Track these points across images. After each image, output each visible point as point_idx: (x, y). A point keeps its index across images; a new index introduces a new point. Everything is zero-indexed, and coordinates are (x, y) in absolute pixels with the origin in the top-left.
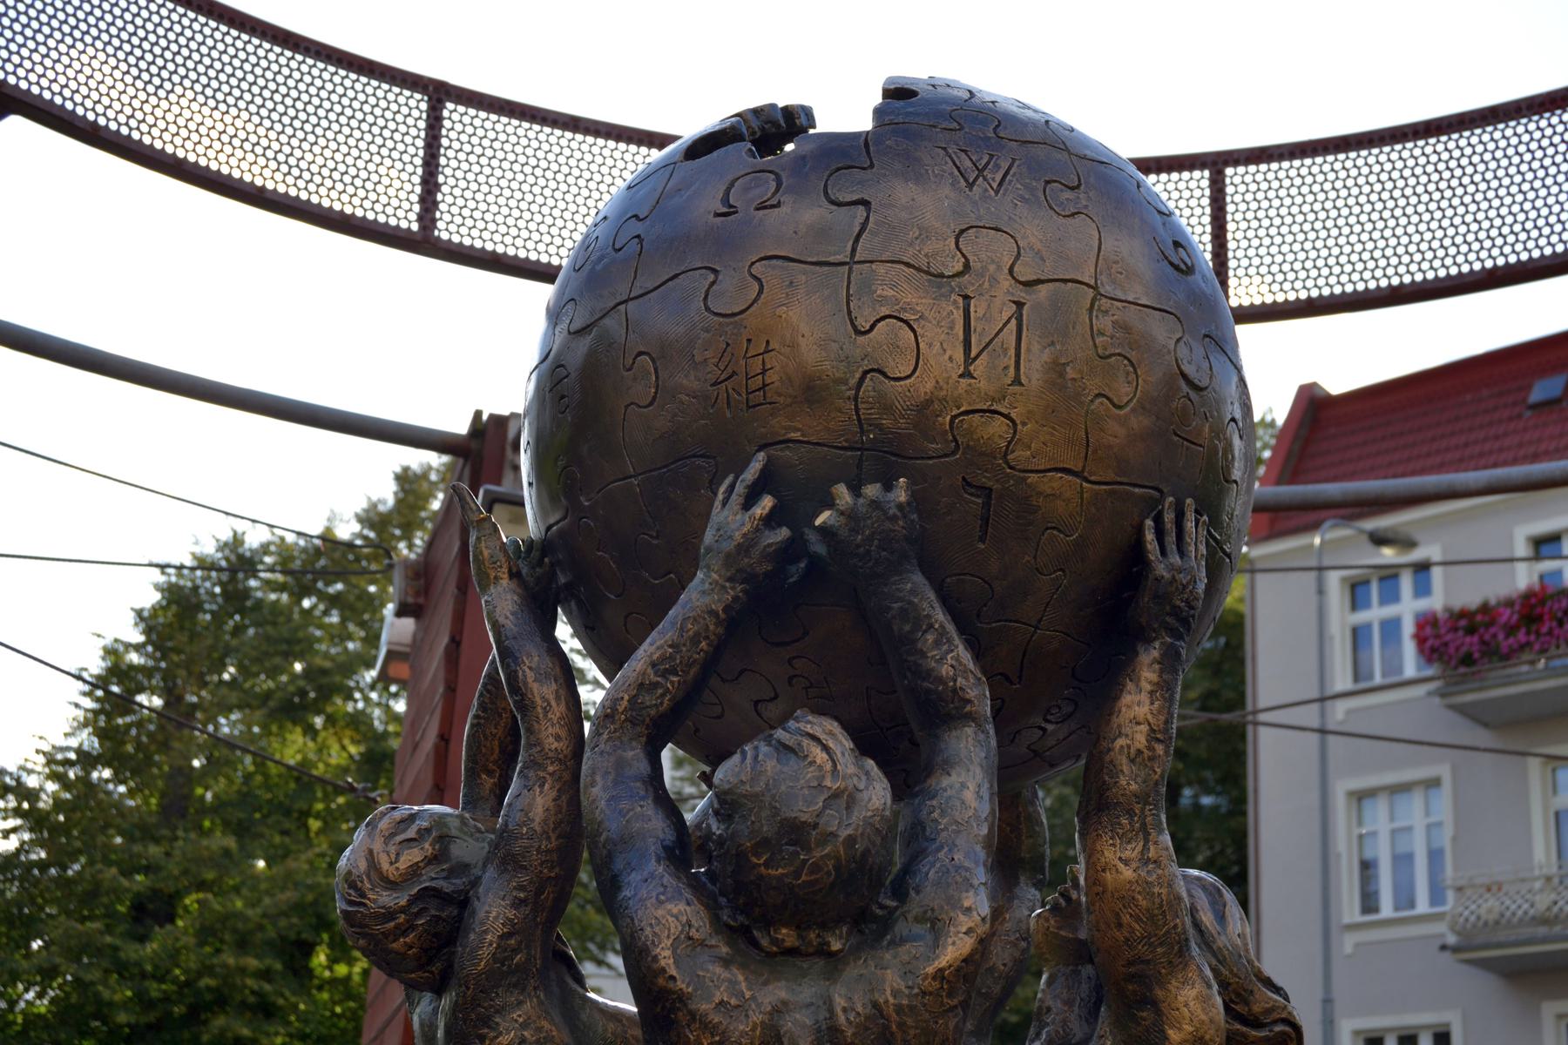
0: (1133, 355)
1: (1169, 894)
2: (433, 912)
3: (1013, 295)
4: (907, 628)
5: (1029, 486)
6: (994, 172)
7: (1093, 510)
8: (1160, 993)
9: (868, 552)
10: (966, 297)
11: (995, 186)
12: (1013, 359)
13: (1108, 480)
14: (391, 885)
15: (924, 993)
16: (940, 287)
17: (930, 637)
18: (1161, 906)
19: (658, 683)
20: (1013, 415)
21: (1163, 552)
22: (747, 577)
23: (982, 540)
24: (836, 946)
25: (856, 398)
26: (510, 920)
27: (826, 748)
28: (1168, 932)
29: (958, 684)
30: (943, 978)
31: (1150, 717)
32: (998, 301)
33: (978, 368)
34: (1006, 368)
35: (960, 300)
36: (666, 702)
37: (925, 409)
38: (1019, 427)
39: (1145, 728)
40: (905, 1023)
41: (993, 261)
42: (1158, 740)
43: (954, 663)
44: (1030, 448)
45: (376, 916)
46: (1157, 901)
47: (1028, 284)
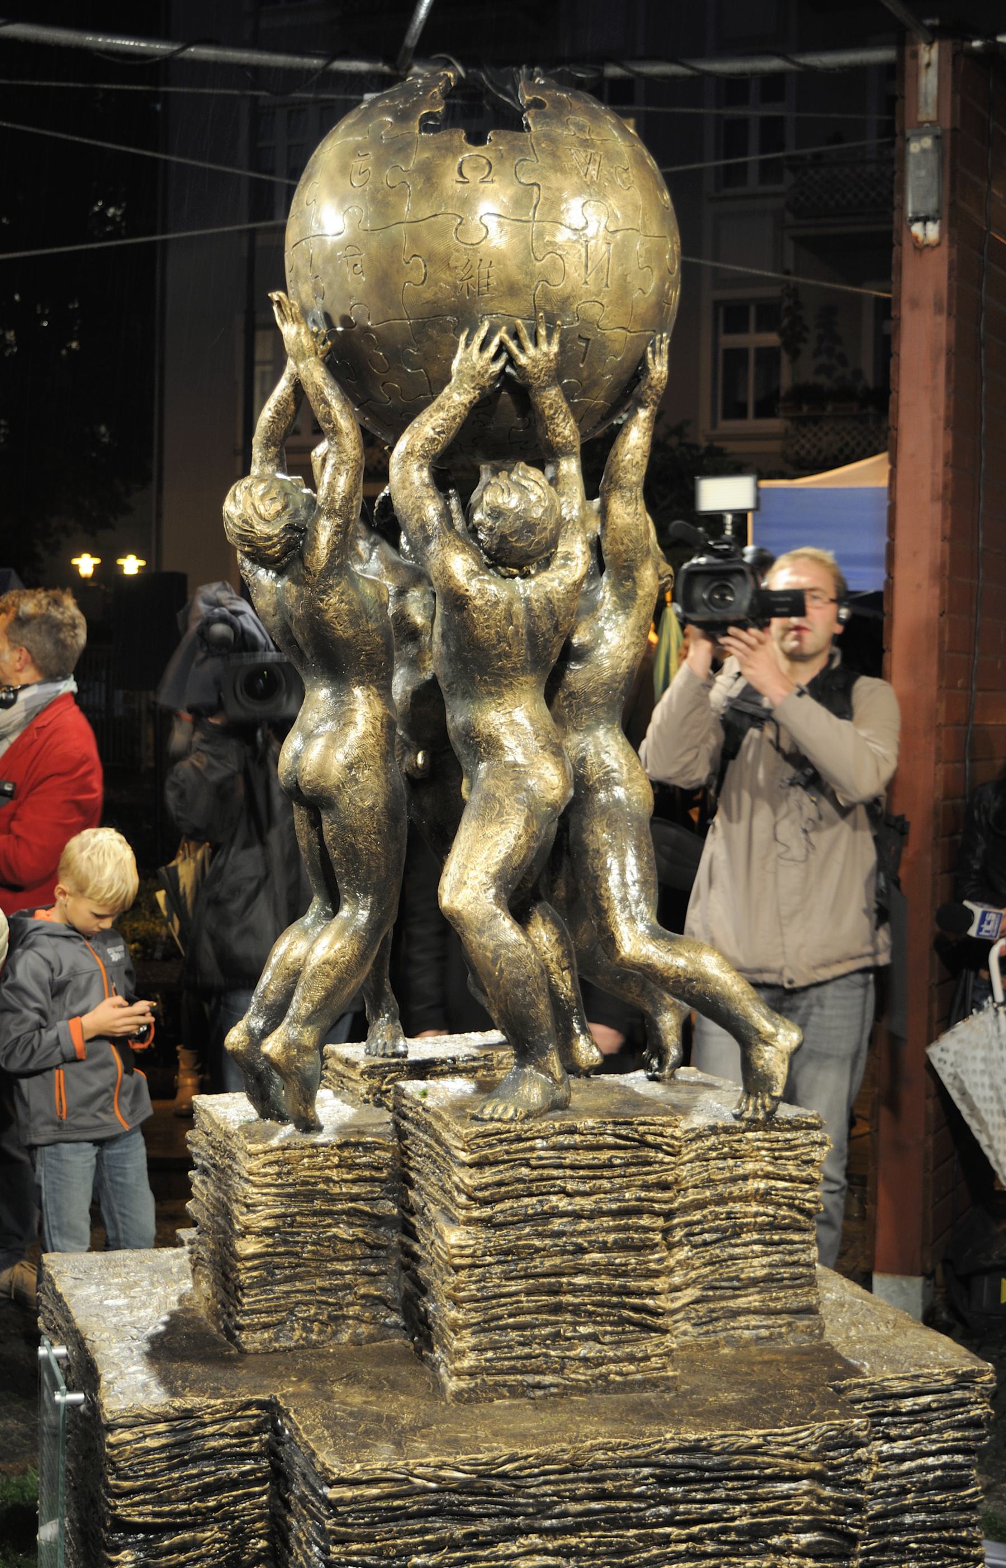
8: (636, 574)
22: (482, 388)
45: (261, 538)
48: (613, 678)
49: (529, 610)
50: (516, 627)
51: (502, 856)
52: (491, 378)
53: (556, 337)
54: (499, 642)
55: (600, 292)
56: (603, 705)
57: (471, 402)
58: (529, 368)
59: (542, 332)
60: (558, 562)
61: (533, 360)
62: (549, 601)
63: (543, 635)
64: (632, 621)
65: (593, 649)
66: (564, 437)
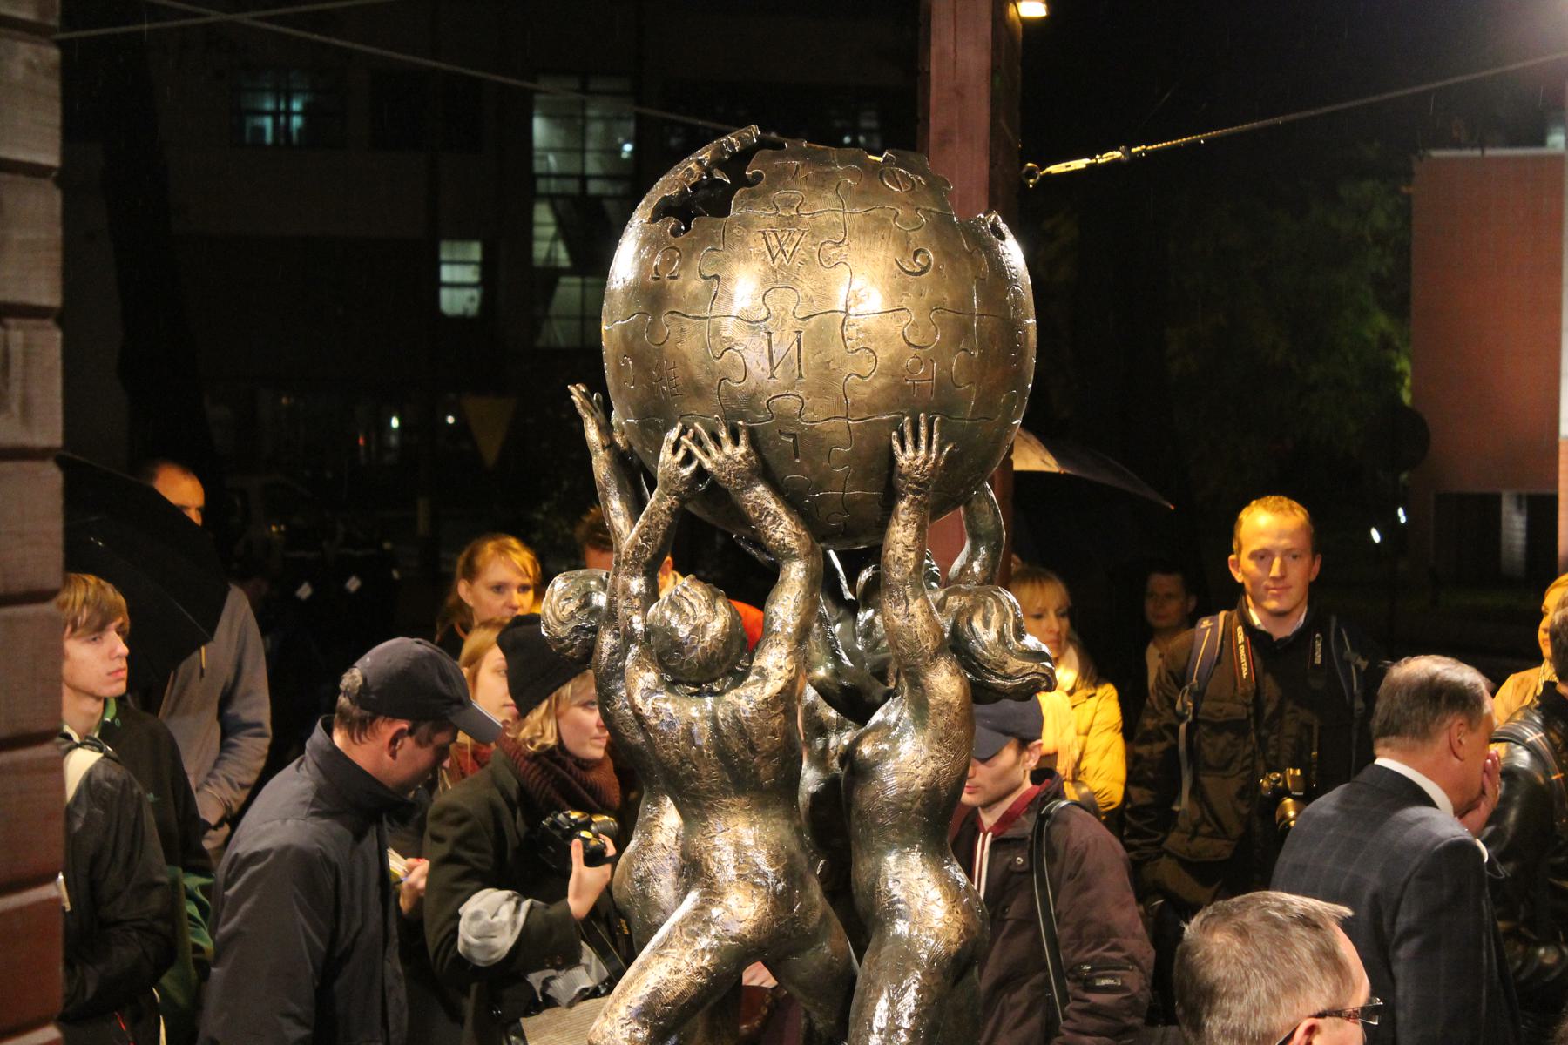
0: (872, 346)
1: (921, 631)
2: (582, 637)
3: (795, 327)
4: (757, 514)
5: (817, 429)
6: (789, 246)
7: (858, 434)
9: (729, 480)
10: (770, 333)
11: (788, 256)
12: (797, 365)
13: (864, 417)
14: (562, 623)
15: (759, 710)
16: (754, 329)
17: (769, 519)
18: (917, 638)
19: (643, 546)
20: (800, 395)
21: (903, 449)
23: (797, 457)
24: (717, 689)
25: (718, 394)
26: (614, 646)
27: (691, 604)
28: (923, 650)
29: (786, 541)
30: (768, 703)
31: (903, 539)
32: (786, 333)
33: (778, 373)
34: (793, 371)
35: (766, 335)
36: (648, 555)
37: (753, 396)
38: (805, 401)
39: (901, 545)
40: (750, 725)
41: (783, 309)
42: (910, 551)
43: (783, 530)
44: (813, 410)
46: (915, 635)
47: (804, 319)
48: (901, 797)
49: (716, 729)
50: (699, 747)
51: (648, 991)
52: (683, 483)
53: (743, 439)
54: (684, 764)
55: (792, 386)
56: (892, 826)
57: (669, 508)
58: (715, 471)
59: (723, 434)
60: (751, 679)
61: (716, 463)
62: (736, 719)
63: (737, 755)
64: (929, 732)
65: (877, 764)
66: (775, 540)
